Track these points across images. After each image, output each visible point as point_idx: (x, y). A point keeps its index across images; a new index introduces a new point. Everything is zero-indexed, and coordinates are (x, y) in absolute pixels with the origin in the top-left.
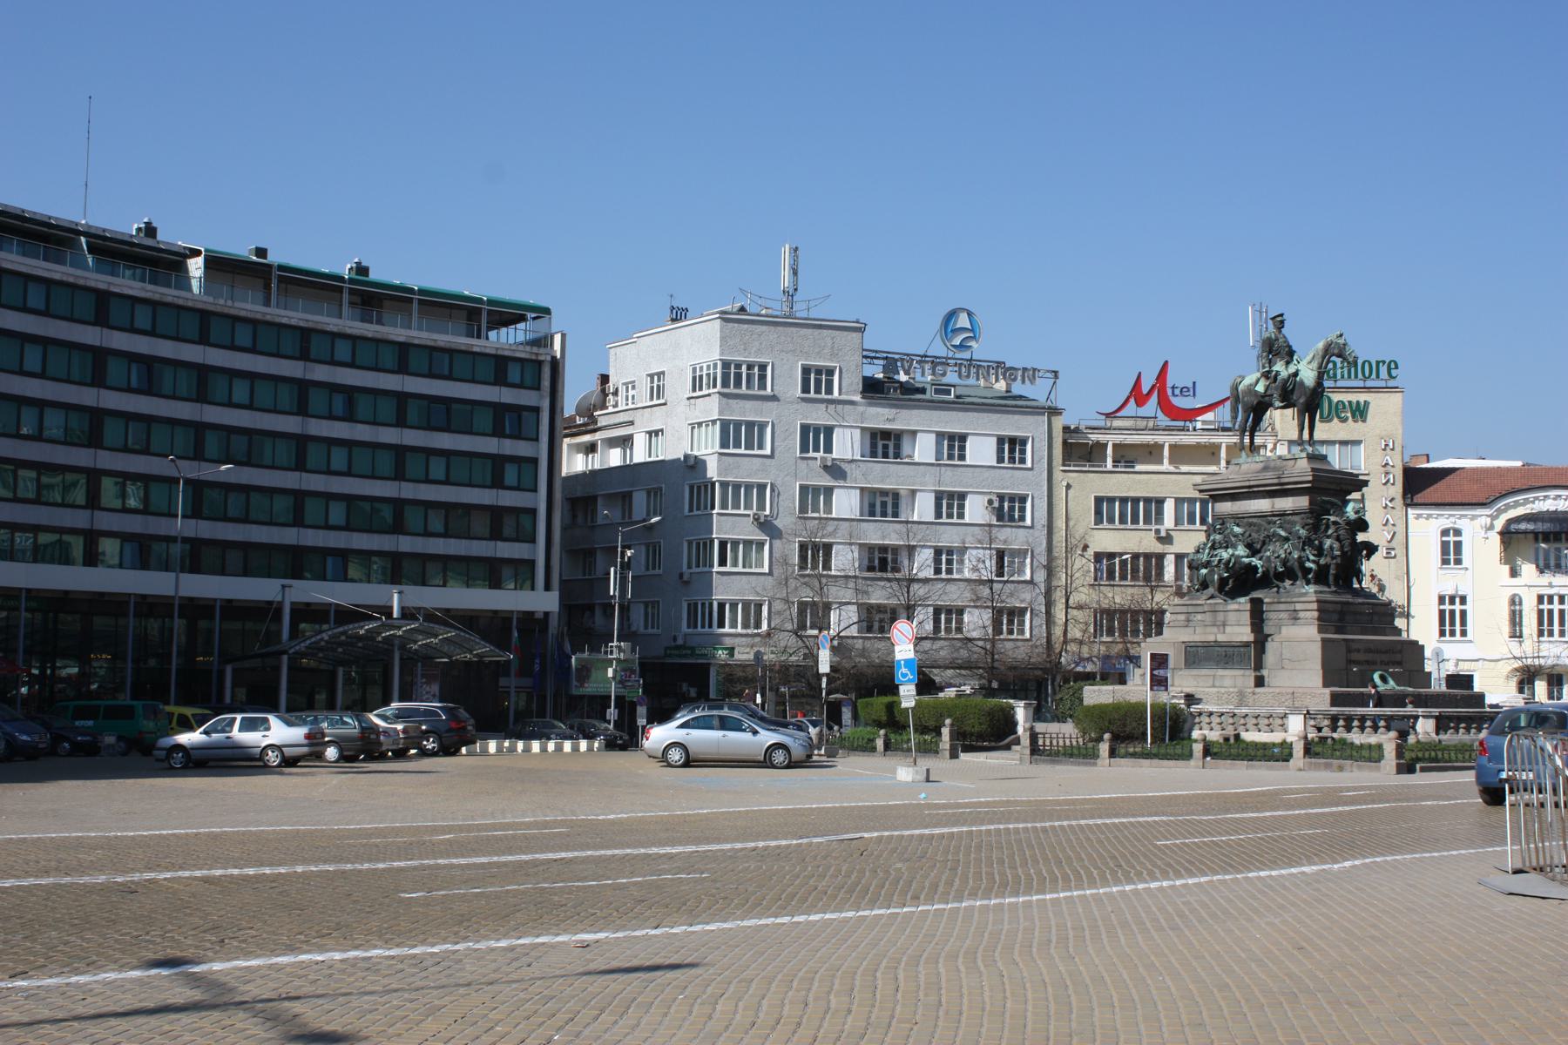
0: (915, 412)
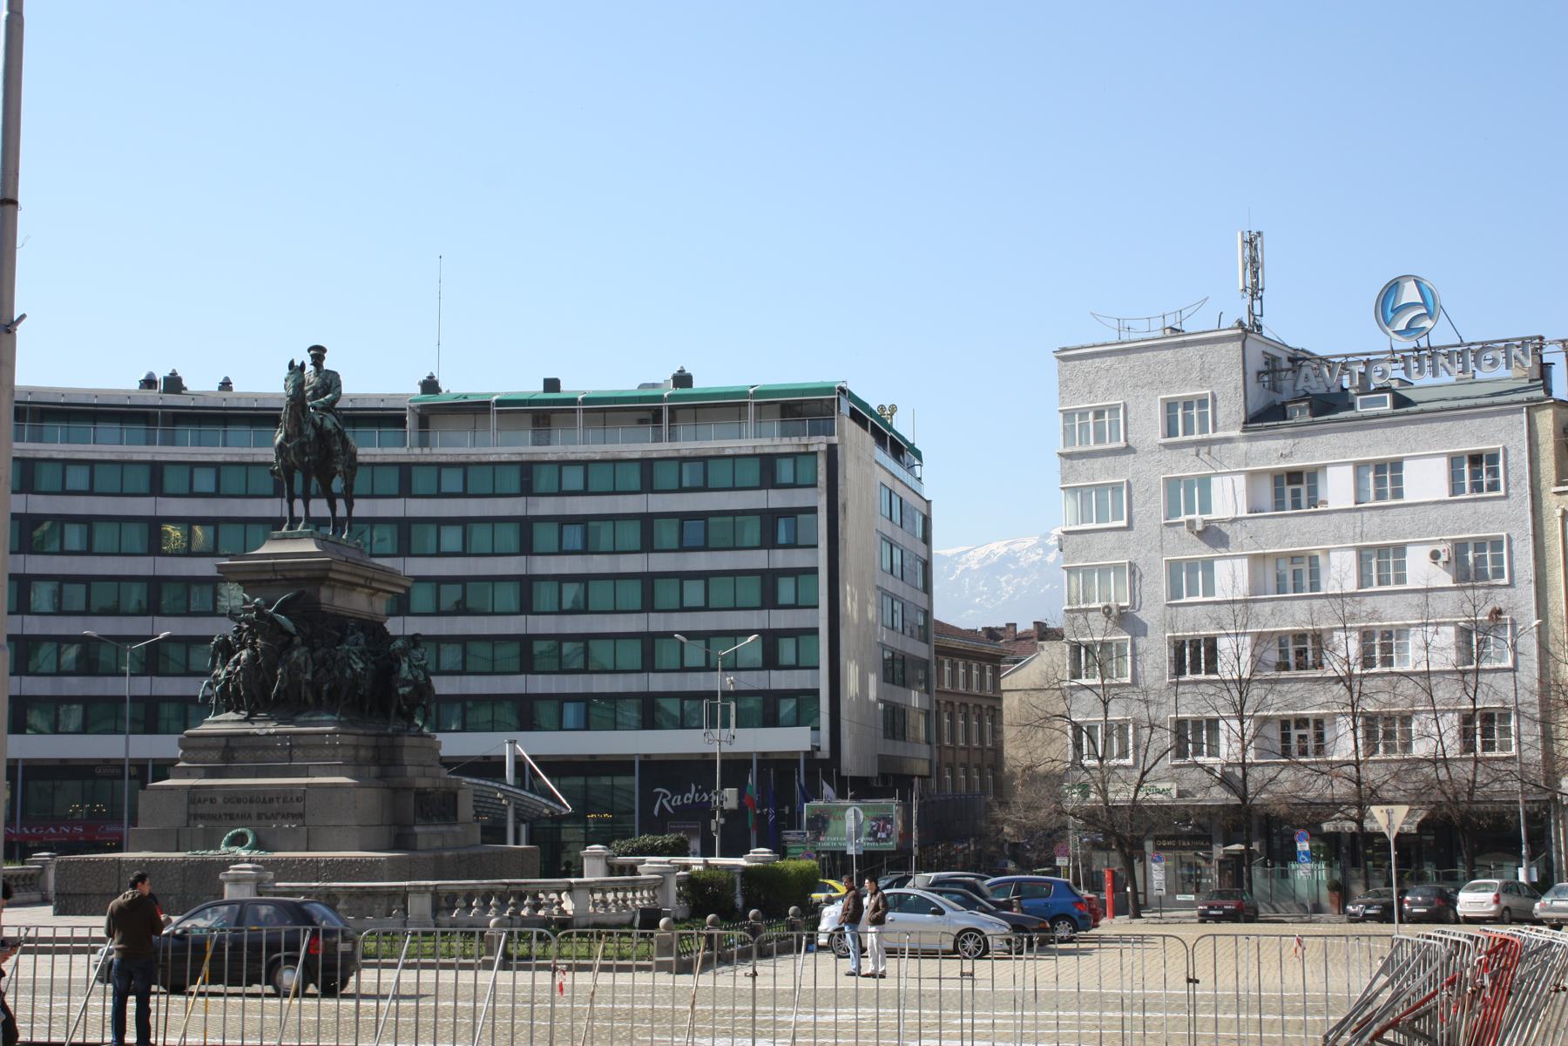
0: (1322, 439)
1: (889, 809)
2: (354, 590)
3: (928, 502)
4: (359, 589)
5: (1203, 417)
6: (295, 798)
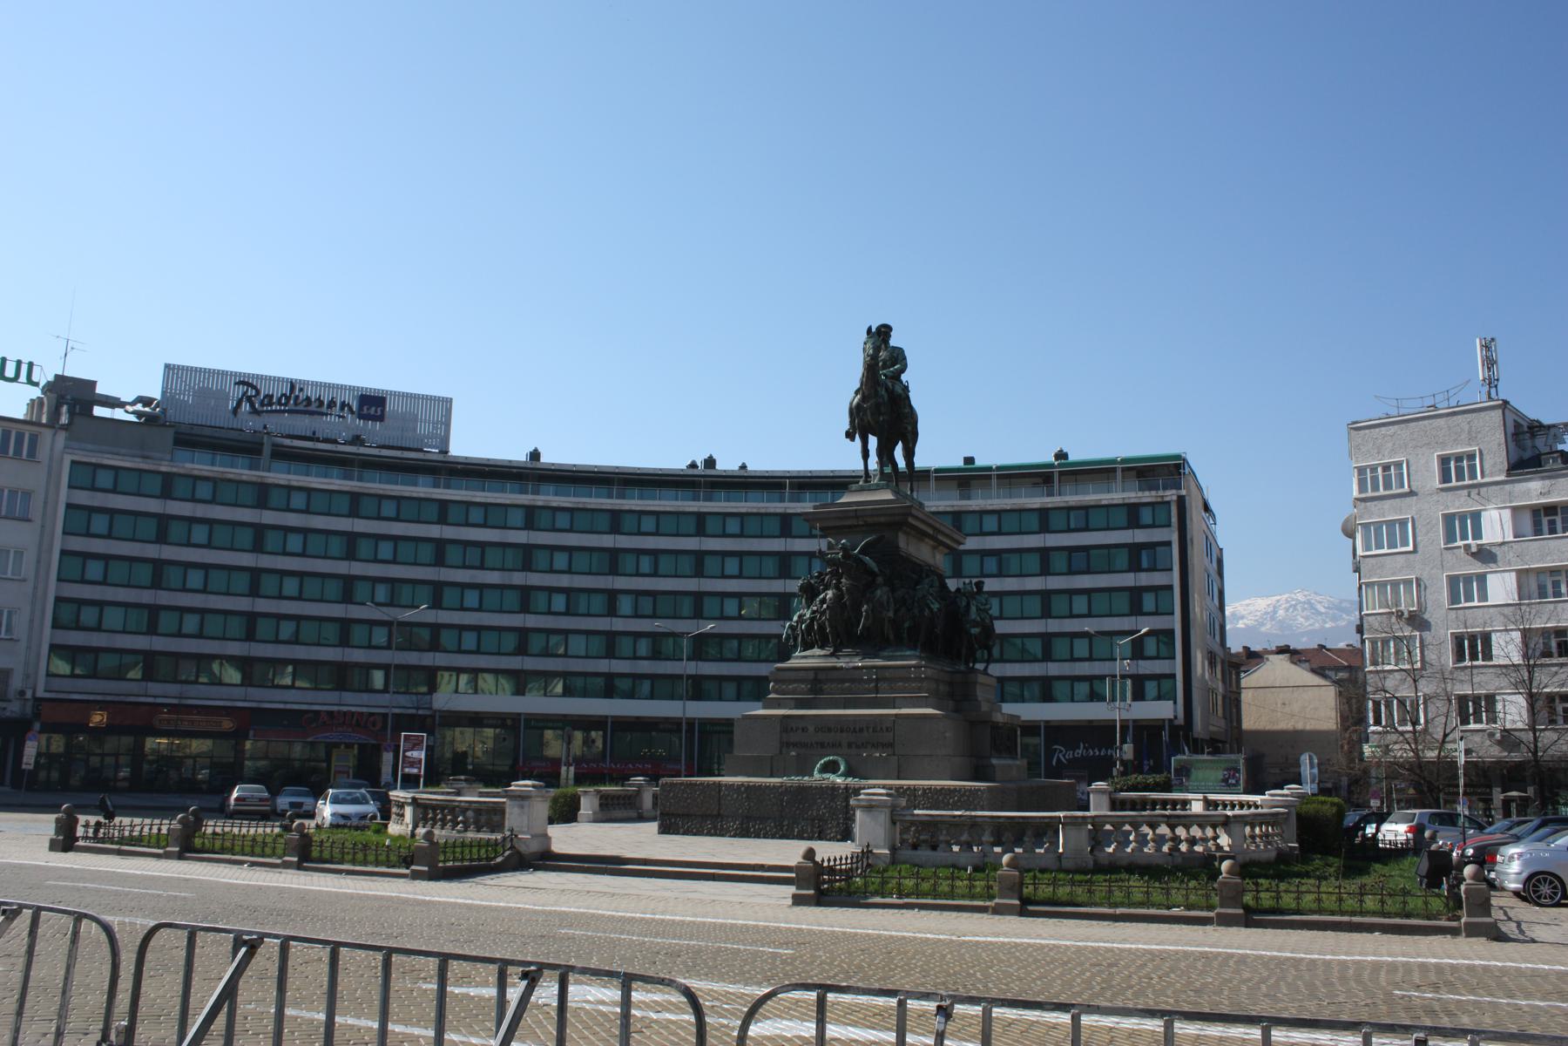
1: (1237, 762)
2: (923, 540)
3: (1221, 550)
4: (927, 540)
5: (1472, 469)
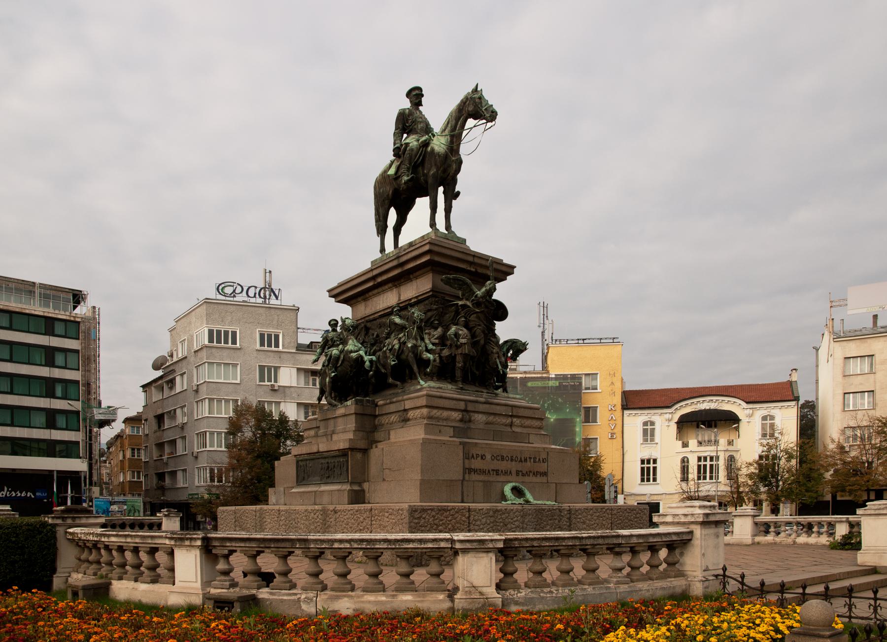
6: (541, 460)
